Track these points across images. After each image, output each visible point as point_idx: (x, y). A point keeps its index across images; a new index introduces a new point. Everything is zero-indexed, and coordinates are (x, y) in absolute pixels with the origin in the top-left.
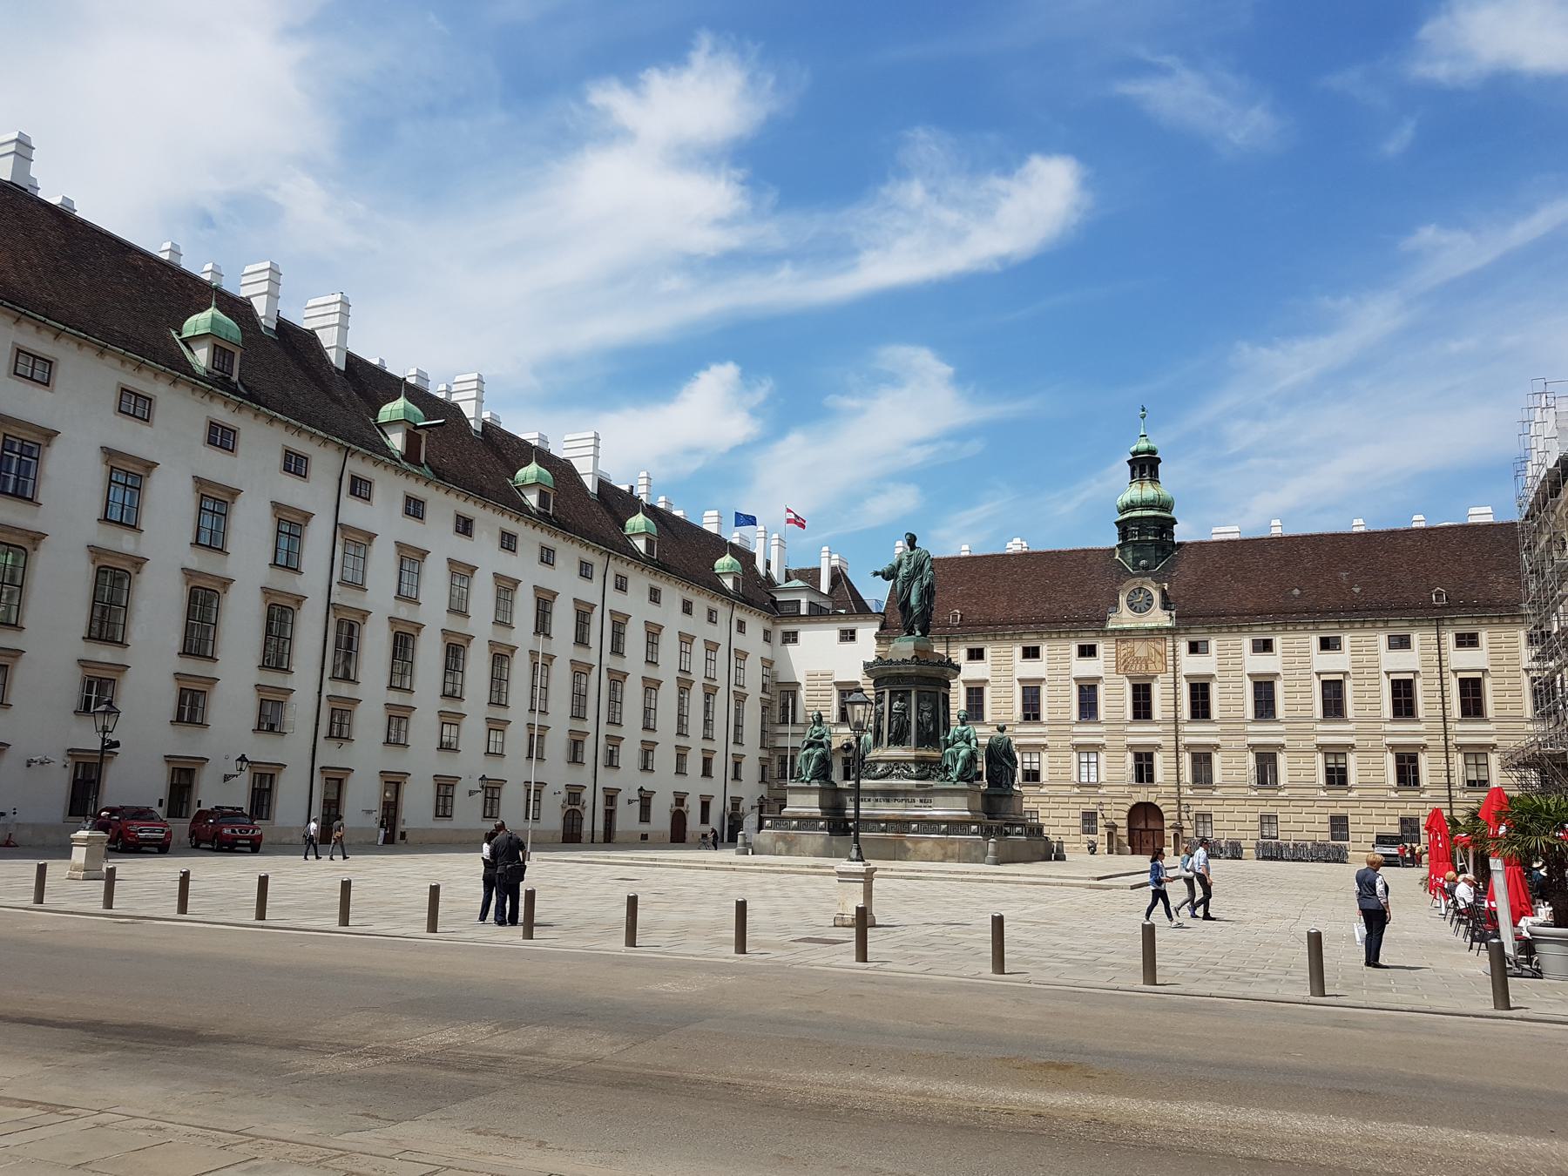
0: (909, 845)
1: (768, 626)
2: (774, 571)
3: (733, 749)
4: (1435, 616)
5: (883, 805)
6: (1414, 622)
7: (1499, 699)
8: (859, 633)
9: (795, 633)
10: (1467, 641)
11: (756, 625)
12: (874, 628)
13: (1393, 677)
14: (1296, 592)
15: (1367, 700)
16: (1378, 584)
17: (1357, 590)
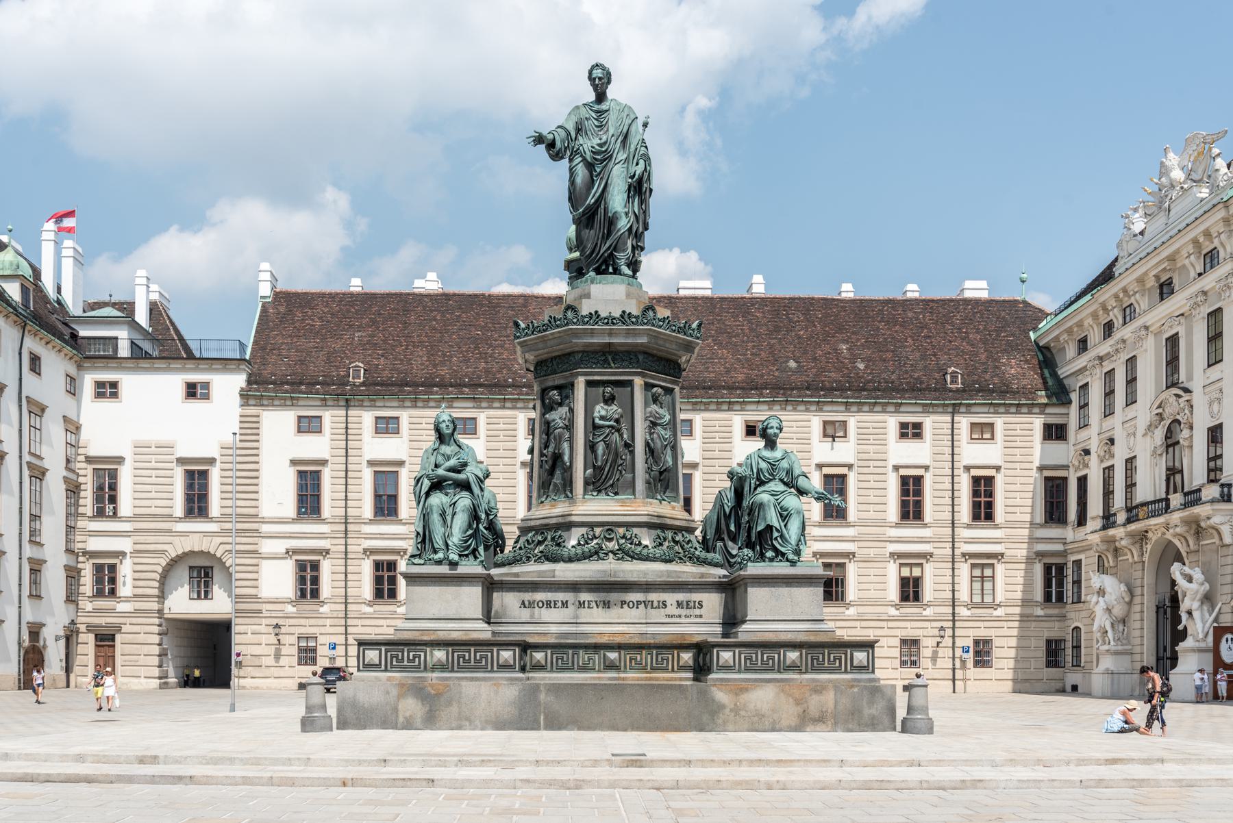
0: (721, 696)
1: (73, 371)
2: (68, 297)
3: (28, 551)
4: (951, 400)
5: (597, 614)
6: (927, 409)
7: (1010, 502)
8: (215, 391)
9: (114, 385)
10: (983, 431)
11: (56, 364)
12: (239, 380)
13: (903, 472)
14: (792, 364)
15: (872, 499)
16: (884, 360)
17: (861, 366)
